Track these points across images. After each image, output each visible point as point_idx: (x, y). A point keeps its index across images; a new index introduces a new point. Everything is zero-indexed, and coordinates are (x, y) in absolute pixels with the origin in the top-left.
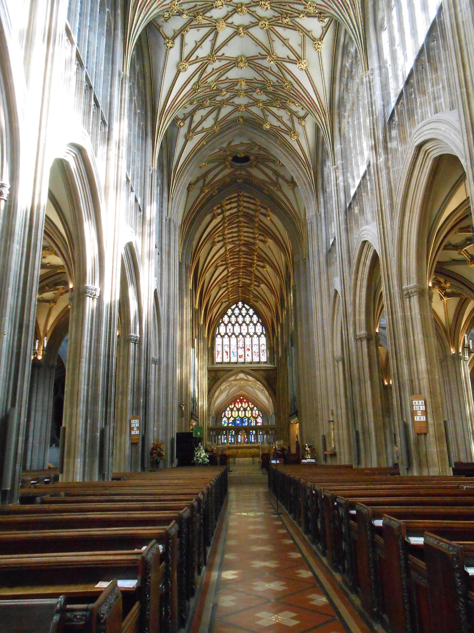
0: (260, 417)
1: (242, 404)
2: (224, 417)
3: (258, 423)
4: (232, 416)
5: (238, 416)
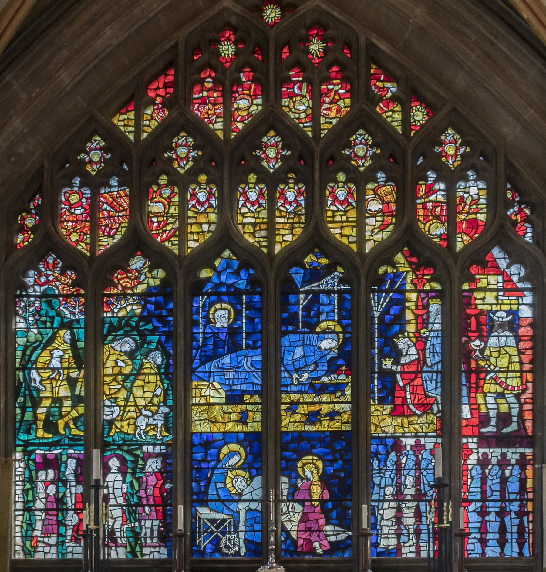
0: (515, 257)
1: (272, 88)
2: (35, 257)
3: (486, 326)
4: (138, 241)
5: (226, 236)
